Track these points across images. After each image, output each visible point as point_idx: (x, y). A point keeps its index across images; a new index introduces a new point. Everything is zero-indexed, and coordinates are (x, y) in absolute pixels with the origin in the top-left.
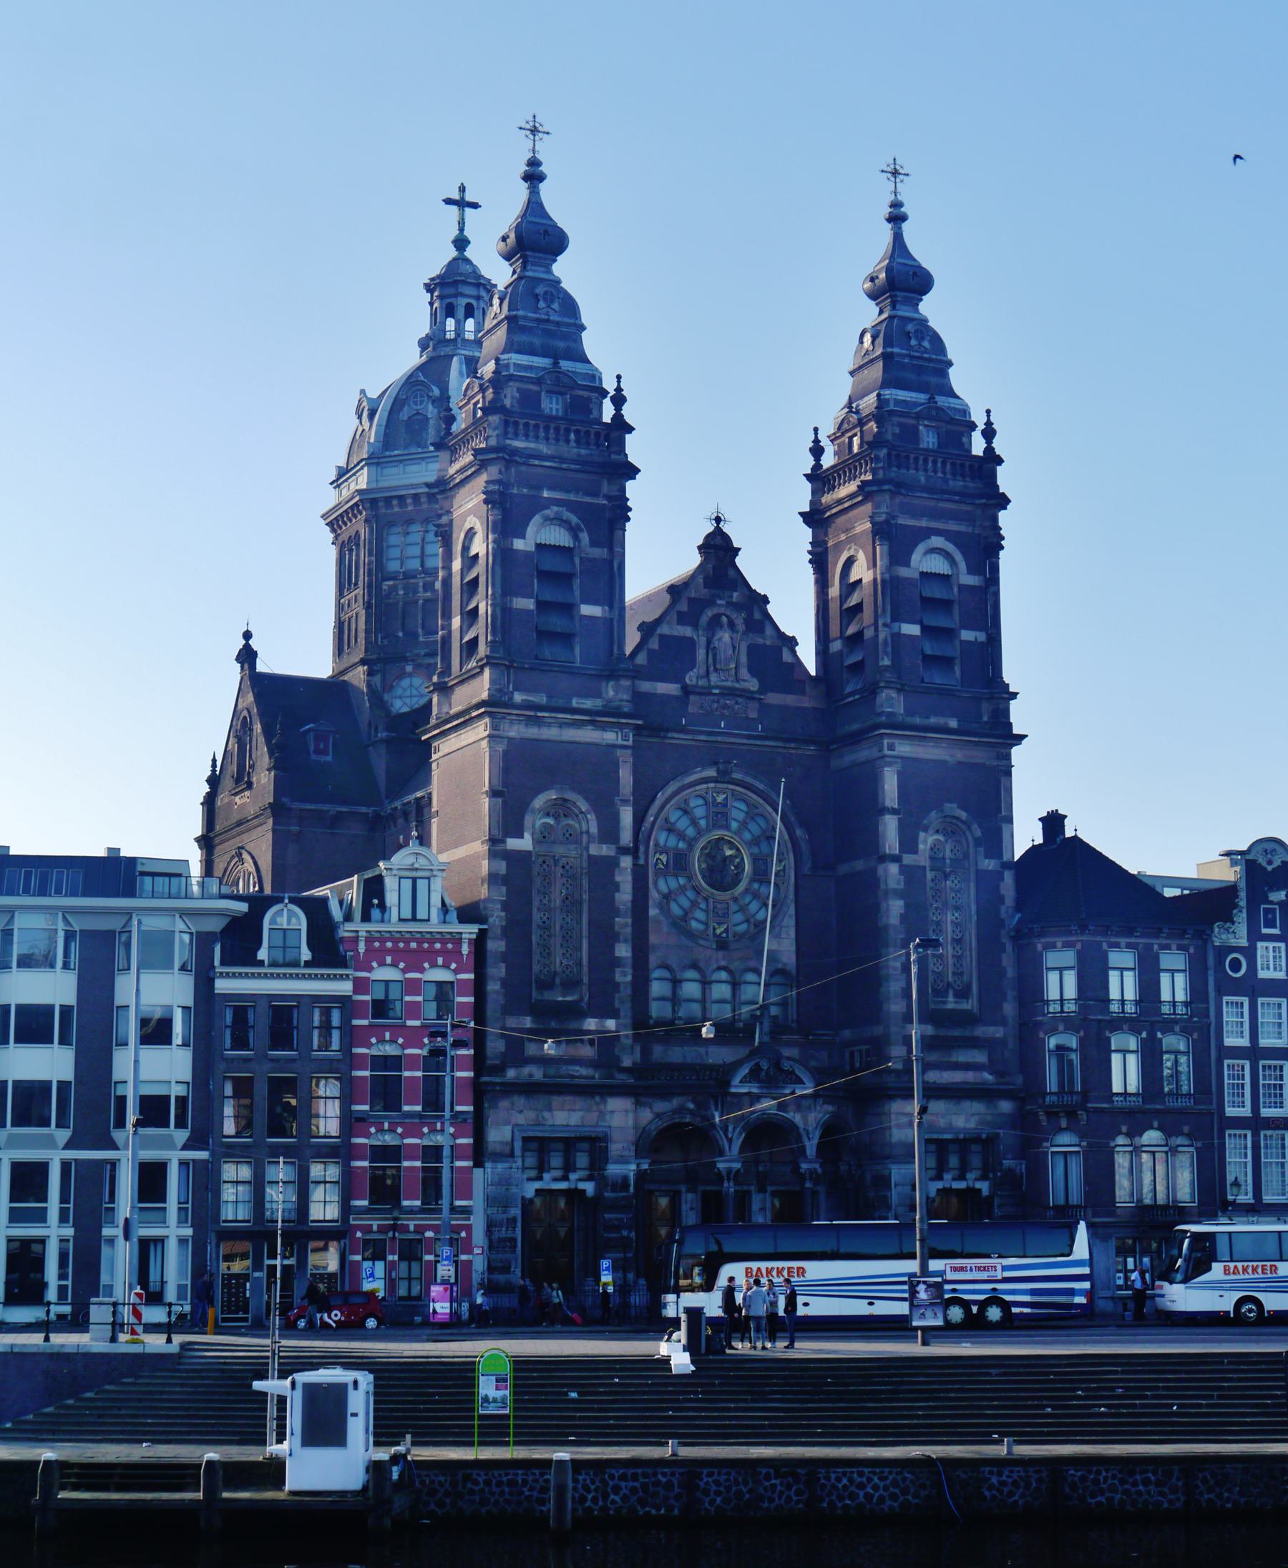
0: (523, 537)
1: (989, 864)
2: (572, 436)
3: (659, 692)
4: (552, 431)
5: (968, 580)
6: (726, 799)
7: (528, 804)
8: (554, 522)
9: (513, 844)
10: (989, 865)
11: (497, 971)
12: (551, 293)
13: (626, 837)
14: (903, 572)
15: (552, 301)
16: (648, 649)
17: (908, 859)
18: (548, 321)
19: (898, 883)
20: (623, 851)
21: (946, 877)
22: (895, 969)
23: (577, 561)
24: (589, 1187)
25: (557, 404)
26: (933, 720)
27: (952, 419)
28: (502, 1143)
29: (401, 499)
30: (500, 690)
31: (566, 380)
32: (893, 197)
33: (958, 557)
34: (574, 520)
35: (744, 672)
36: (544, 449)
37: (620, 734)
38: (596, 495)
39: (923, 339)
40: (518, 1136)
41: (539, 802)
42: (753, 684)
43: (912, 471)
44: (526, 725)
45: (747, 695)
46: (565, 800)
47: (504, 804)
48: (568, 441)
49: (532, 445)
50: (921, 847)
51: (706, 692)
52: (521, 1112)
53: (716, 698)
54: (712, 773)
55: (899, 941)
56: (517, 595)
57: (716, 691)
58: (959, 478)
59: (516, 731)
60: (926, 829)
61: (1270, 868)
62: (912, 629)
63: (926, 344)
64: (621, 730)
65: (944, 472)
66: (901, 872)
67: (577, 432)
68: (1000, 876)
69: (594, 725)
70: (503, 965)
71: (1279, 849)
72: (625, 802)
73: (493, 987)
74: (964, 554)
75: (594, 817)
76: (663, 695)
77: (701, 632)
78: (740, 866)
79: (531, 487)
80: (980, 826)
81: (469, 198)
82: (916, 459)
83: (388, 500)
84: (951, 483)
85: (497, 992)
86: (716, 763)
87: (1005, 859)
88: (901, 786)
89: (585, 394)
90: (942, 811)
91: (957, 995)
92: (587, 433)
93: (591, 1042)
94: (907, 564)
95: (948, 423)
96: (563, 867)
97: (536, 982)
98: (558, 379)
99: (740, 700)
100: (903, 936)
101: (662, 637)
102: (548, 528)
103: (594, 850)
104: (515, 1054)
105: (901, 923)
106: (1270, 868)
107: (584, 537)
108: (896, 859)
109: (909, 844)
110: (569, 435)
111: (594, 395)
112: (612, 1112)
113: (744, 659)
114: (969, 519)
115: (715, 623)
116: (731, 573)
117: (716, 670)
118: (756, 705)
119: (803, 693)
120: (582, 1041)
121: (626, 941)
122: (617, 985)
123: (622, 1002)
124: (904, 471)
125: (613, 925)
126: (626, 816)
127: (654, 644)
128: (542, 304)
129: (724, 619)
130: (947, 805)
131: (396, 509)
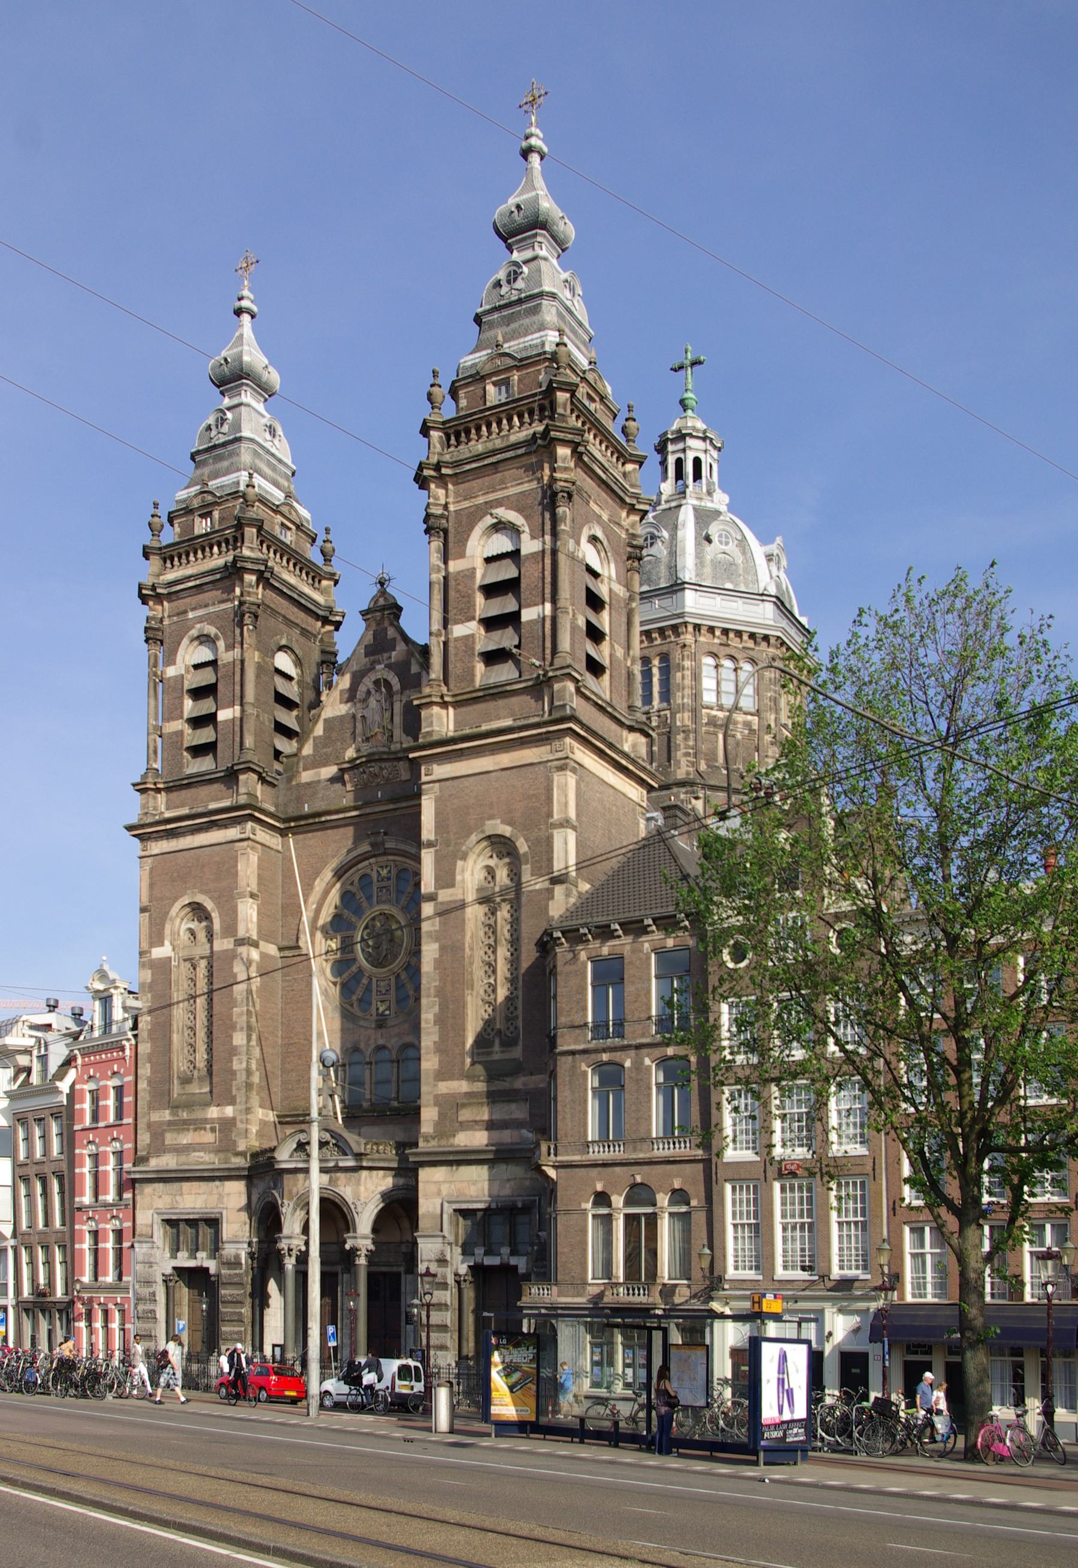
9: (158, 953)
11: (145, 1070)
17: (444, 895)
22: (427, 1022)
24: (212, 1265)
28: (146, 1225)
35: (398, 733)
40: (157, 1219)
50: (458, 878)
52: (160, 1197)
55: (432, 991)
64: (239, 823)
68: (549, 894)
69: (217, 825)
70: (148, 1065)
73: (142, 1085)
80: (526, 840)
85: (144, 1090)
88: (438, 814)
90: (483, 832)
91: (502, 1044)
93: (213, 1130)
97: (179, 1077)
100: (437, 983)
104: (159, 1147)
105: (435, 969)
108: (432, 898)
109: (446, 879)
112: (229, 1194)
120: (205, 1129)
121: (242, 1029)
122: (233, 1073)
123: (238, 1089)
125: (230, 1017)
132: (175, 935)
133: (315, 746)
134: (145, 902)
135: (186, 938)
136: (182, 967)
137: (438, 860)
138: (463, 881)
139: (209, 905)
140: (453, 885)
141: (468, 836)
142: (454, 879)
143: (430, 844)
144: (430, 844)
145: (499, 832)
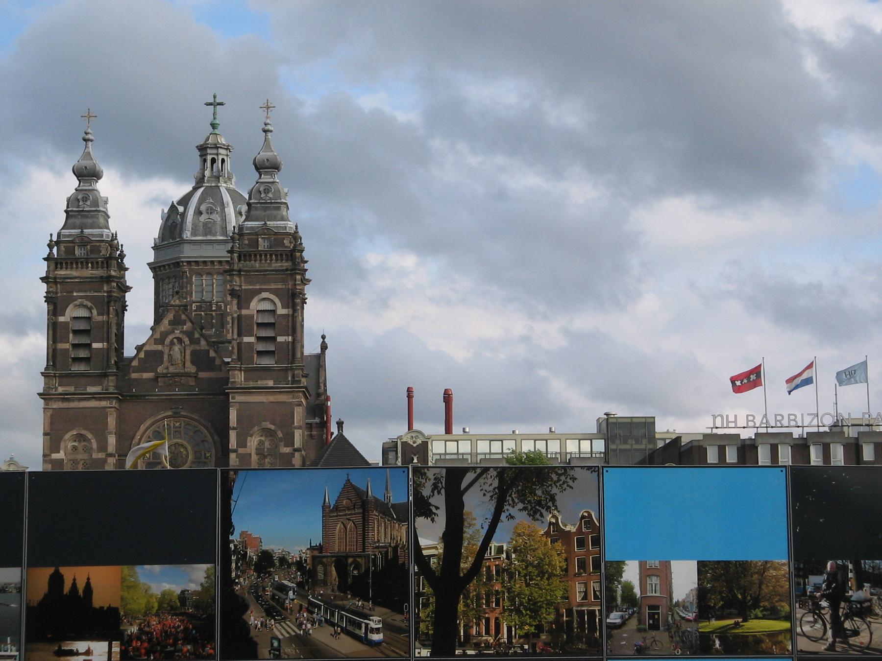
0: (64, 315)
1: (287, 450)
2: (90, 265)
3: (144, 377)
4: (79, 264)
5: (281, 311)
6: (180, 424)
7: (63, 438)
8: (81, 306)
9: (55, 456)
10: (286, 450)
12: (86, 198)
13: (111, 448)
14: (244, 312)
15: (86, 201)
16: (139, 358)
17: (241, 450)
18: (83, 211)
19: (236, 462)
20: (111, 455)
21: (265, 457)
23: (92, 322)
25: (84, 250)
26: (260, 383)
27: (276, 233)
29: (164, 266)
30: (49, 388)
31: (86, 239)
32: (264, 120)
33: (277, 300)
34: (89, 304)
35: (188, 364)
36: (75, 273)
37: (108, 402)
38: (101, 292)
39: (268, 193)
41: (67, 436)
42: (193, 369)
43: (253, 262)
44: (63, 402)
45: (188, 375)
46: (82, 434)
47: (50, 438)
48: (87, 268)
49: (68, 272)
50: (248, 444)
51: (165, 376)
53: (170, 378)
54: (170, 413)
56: (60, 342)
57: (169, 375)
58: (279, 262)
59: (56, 405)
60: (251, 436)
61: (415, 445)
62: (252, 339)
63: (270, 195)
64: (109, 400)
65: (271, 260)
66: (237, 458)
67: (92, 263)
71: (420, 436)
72: (111, 433)
74: (280, 300)
75: (95, 440)
76: (146, 379)
77: (165, 347)
78: (187, 456)
79: (67, 292)
80: (282, 432)
81: (218, 100)
82: (255, 255)
83: (160, 267)
84: (273, 265)
86: (172, 409)
87: (295, 447)
89: (98, 244)
90: (261, 426)
92: (97, 263)
94: (248, 308)
95: (274, 235)
96: (83, 464)
98: (82, 239)
99: (183, 378)
101: (146, 352)
102: (78, 309)
103: (94, 456)
106: (415, 445)
107: (95, 312)
108: (235, 451)
109: (242, 443)
110: (88, 265)
111: (102, 244)
113: (188, 357)
114: (284, 281)
115: (172, 343)
116: (183, 317)
117: (172, 365)
118: (193, 379)
119: (221, 370)
124: (248, 263)
126: (112, 440)
127: (142, 355)
128: (81, 203)
129: (175, 340)
130: (264, 423)
131: (164, 272)
132: (66, 447)
133: (139, 362)
134: (48, 430)
135: (70, 449)
136: (69, 464)
137: (238, 436)
138: (251, 446)
139: (90, 436)
140: (246, 447)
141: (253, 427)
142: (246, 445)
143: (234, 429)
144: (234, 429)
145: (269, 427)
